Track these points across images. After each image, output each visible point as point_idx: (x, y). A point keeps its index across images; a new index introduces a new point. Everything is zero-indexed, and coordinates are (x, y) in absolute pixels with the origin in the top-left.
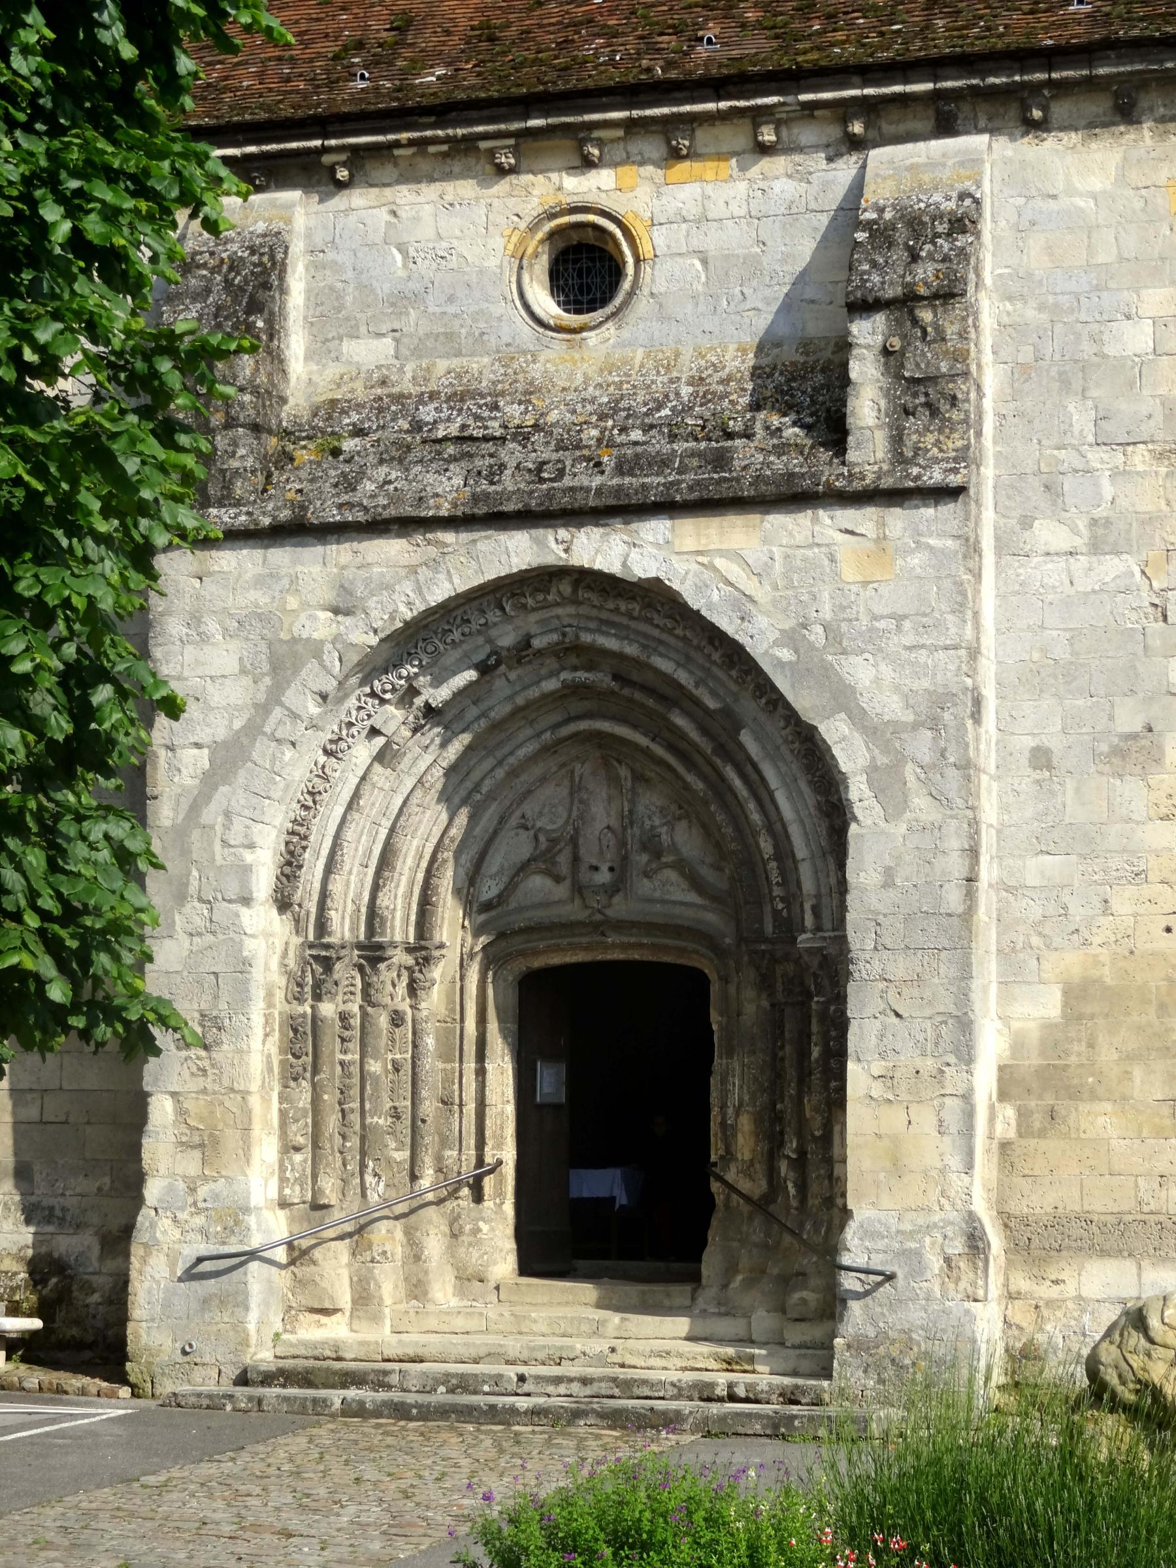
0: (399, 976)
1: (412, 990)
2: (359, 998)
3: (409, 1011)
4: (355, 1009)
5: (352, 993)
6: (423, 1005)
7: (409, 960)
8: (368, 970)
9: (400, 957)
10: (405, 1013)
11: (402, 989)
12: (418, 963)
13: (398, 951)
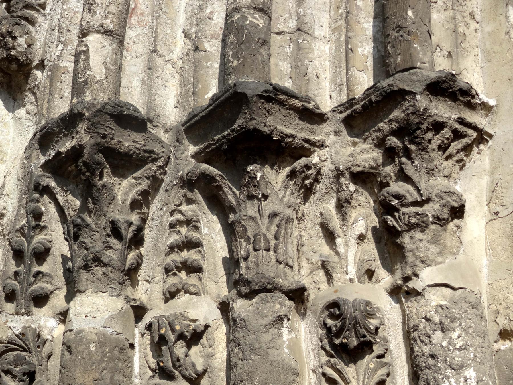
0: (342, 206)
1: (389, 242)
2: (216, 282)
3: (390, 311)
4: (202, 310)
5: (194, 269)
6: (427, 276)
7: (366, 154)
8: (231, 194)
9: (337, 150)
10: (369, 311)
11: (355, 250)
12: (390, 154)
13: (325, 133)
